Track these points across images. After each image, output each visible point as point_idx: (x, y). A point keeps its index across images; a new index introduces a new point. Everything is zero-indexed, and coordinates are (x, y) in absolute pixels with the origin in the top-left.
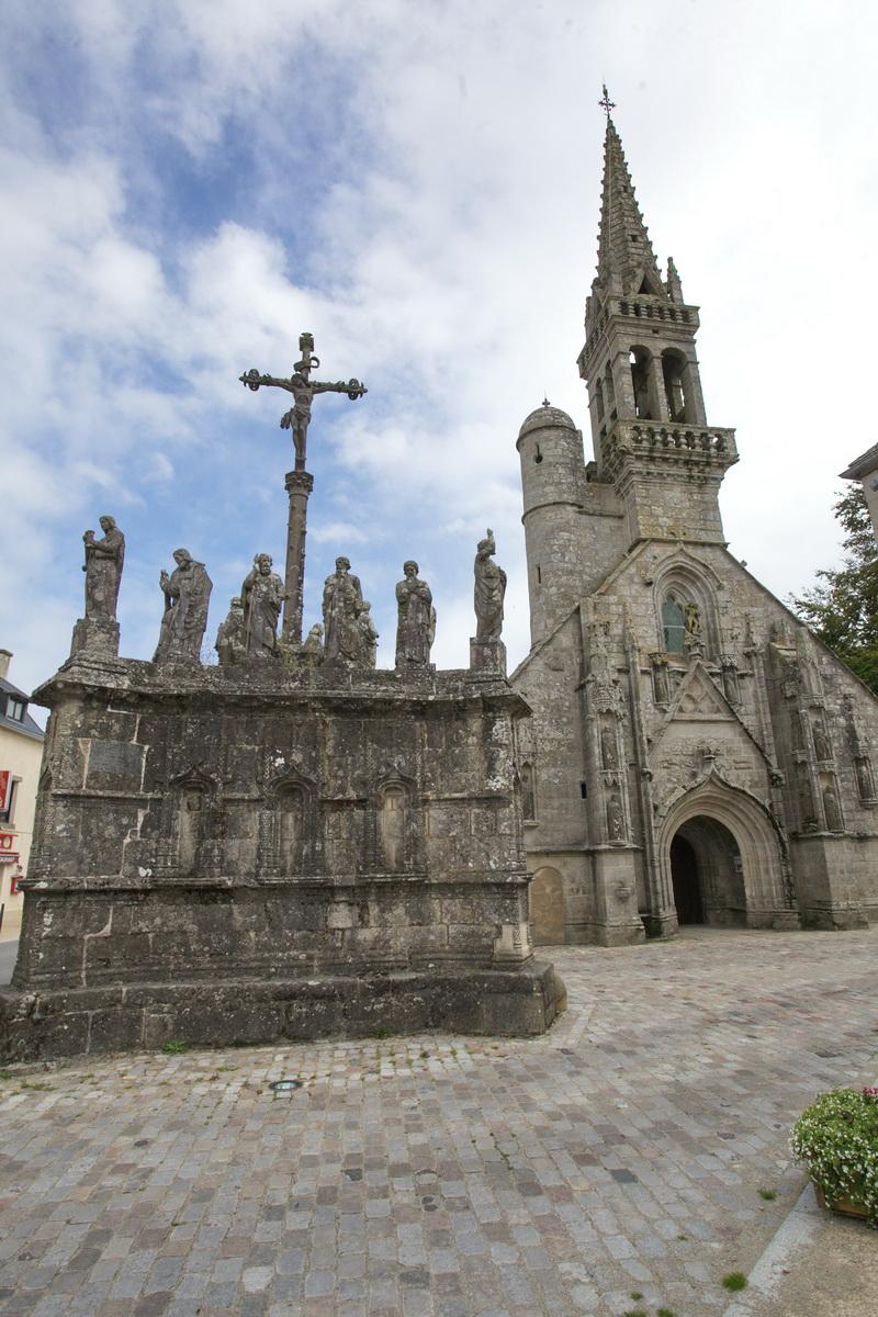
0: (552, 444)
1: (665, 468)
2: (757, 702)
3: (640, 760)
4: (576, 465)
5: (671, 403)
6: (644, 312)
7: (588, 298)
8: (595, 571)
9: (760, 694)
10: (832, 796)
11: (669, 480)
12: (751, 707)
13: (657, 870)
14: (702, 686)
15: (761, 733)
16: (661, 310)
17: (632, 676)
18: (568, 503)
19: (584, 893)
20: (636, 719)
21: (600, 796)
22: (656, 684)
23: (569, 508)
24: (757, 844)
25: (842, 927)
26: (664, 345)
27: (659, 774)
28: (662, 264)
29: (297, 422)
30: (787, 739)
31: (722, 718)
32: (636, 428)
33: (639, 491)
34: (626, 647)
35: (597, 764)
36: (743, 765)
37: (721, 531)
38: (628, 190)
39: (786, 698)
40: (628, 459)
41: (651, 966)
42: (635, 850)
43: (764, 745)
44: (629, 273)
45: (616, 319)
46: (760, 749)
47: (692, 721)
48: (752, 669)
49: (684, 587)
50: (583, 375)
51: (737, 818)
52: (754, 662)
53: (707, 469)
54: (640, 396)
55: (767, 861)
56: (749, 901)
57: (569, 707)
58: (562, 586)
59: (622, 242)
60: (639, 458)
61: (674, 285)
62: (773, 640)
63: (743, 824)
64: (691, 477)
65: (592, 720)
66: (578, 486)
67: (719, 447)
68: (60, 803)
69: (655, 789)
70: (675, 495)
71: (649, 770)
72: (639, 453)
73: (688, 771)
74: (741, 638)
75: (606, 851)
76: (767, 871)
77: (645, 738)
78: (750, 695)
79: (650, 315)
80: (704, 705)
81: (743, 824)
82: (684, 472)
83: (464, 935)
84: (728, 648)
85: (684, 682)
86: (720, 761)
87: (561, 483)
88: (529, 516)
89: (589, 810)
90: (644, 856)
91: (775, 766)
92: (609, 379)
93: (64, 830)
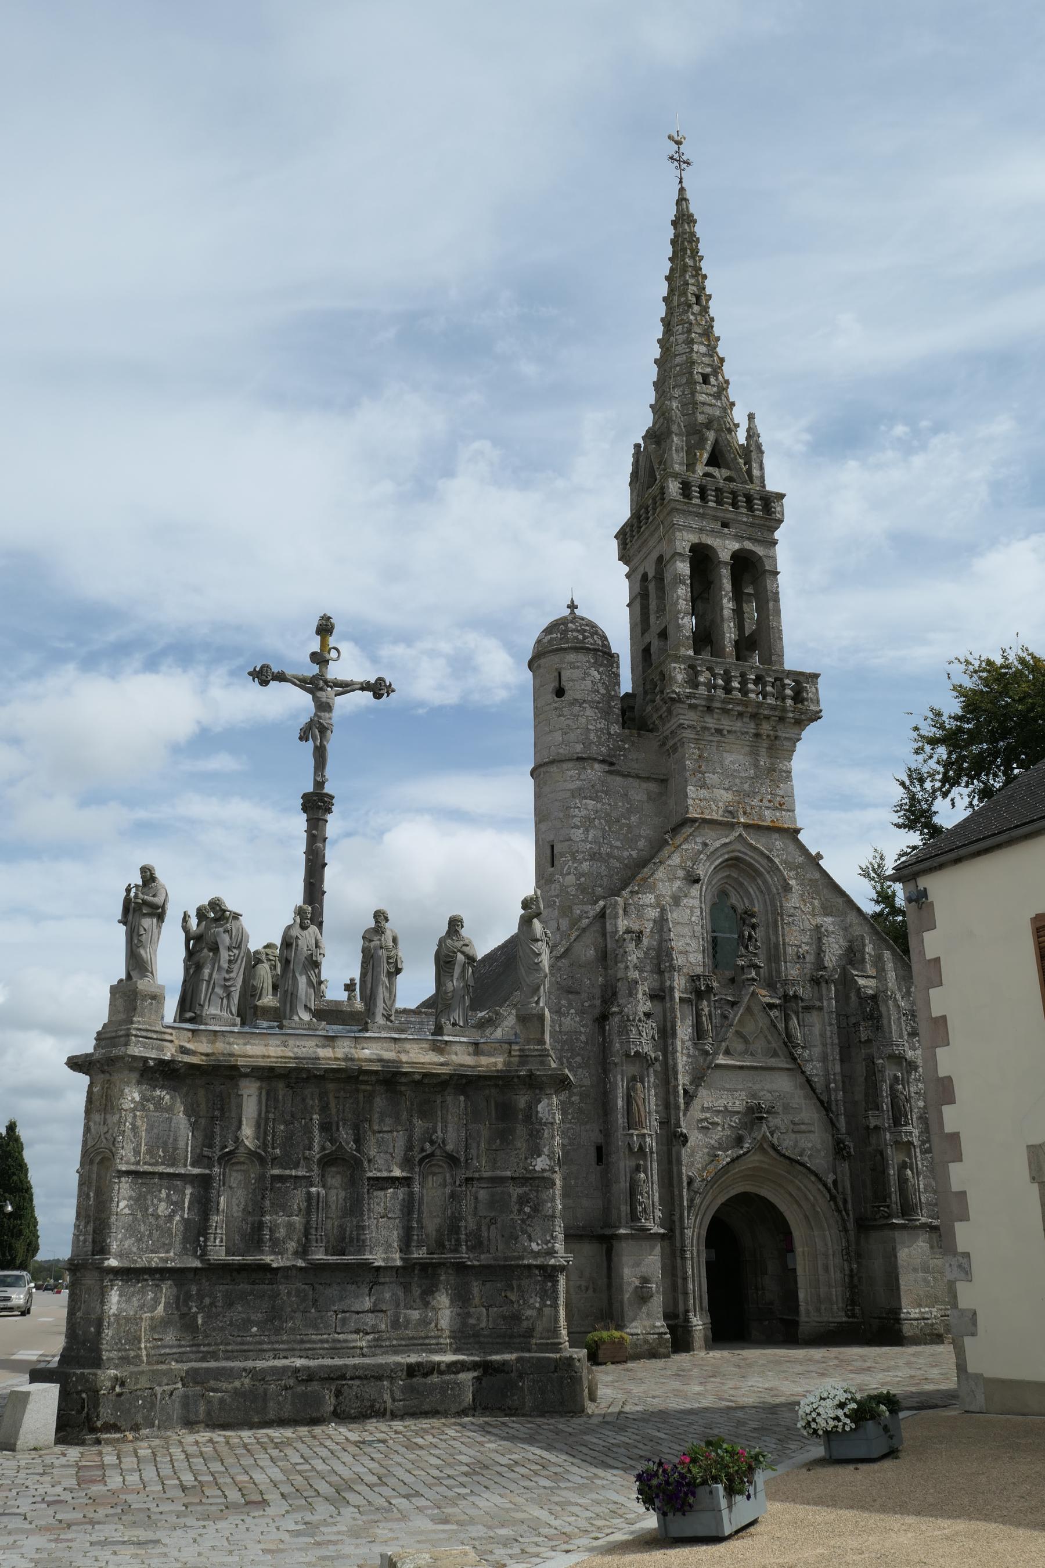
0: (578, 673)
1: (726, 723)
2: (824, 1045)
3: (673, 1117)
4: (608, 703)
5: (739, 613)
6: (711, 496)
7: (637, 446)
8: (626, 854)
9: (828, 1034)
10: (909, 1172)
11: (731, 738)
12: (817, 1051)
13: (689, 1262)
15: (827, 1086)
16: (734, 494)
17: (668, 1005)
18: (595, 759)
19: (594, 1291)
20: (670, 1062)
21: (622, 1165)
22: (698, 1016)
23: (597, 766)
24: (816, 1233)
25: (915, 1341)
26: (736, 546)
27: (695, 1138)
28: (739, 415)
29: (316, 731)
30: (859, 1096)
31: (780, 1065)
33: (691, 751)
34: (661, 960)
35: (620, 1121)
36: (803, 1127)
37: (793, 811)
38: (701, 298)
39: (860, 1041)
40: (678, 708)
41: (679, 1375)
42: (662, 1236)
43: (829, 1102)
44: (695, 433)
45: (673, 505)
46: (825, 1106)
47: (741, 1068)
48: (821, 1000)
49: (741, 884)
50: (624, 558)
51: (791, 1195)
52: (824, 991)
53: (780, 727)
54: (699, 603)
55: (826, 1256)
56: (802, 1308)
57: (586, 1043)
58: (583, 875)
59: (687, 362)
60: (692, 707)
61: (754, 455)
62: (851, 962)
63: (800, 1205)
65: (616, 1064)
66: (609, 734)
67: (798, 696)
68: (123, 1179)
69: (692, 1155)
70: (735, 758)
71: (685, 1131)
72: (693, 701)
74: (810, 958)
75: (626, 1236)
76: (826, 1269)
77: (680, 1087)
78: (815, 1034)
79: (719, 502)
80: (759, 1045)
81: (800, 1205)
82: (751, 728)
83: (504, 1318)
84: (793, 972)
85: (736, 1015)
86: (774, 1121)
87: (590, 726)
88: (543, 769)
89: (606, 1183)
90: (672, 1244)
91: (843, 1130)
92: (660, 578)
93: (127, 1206)
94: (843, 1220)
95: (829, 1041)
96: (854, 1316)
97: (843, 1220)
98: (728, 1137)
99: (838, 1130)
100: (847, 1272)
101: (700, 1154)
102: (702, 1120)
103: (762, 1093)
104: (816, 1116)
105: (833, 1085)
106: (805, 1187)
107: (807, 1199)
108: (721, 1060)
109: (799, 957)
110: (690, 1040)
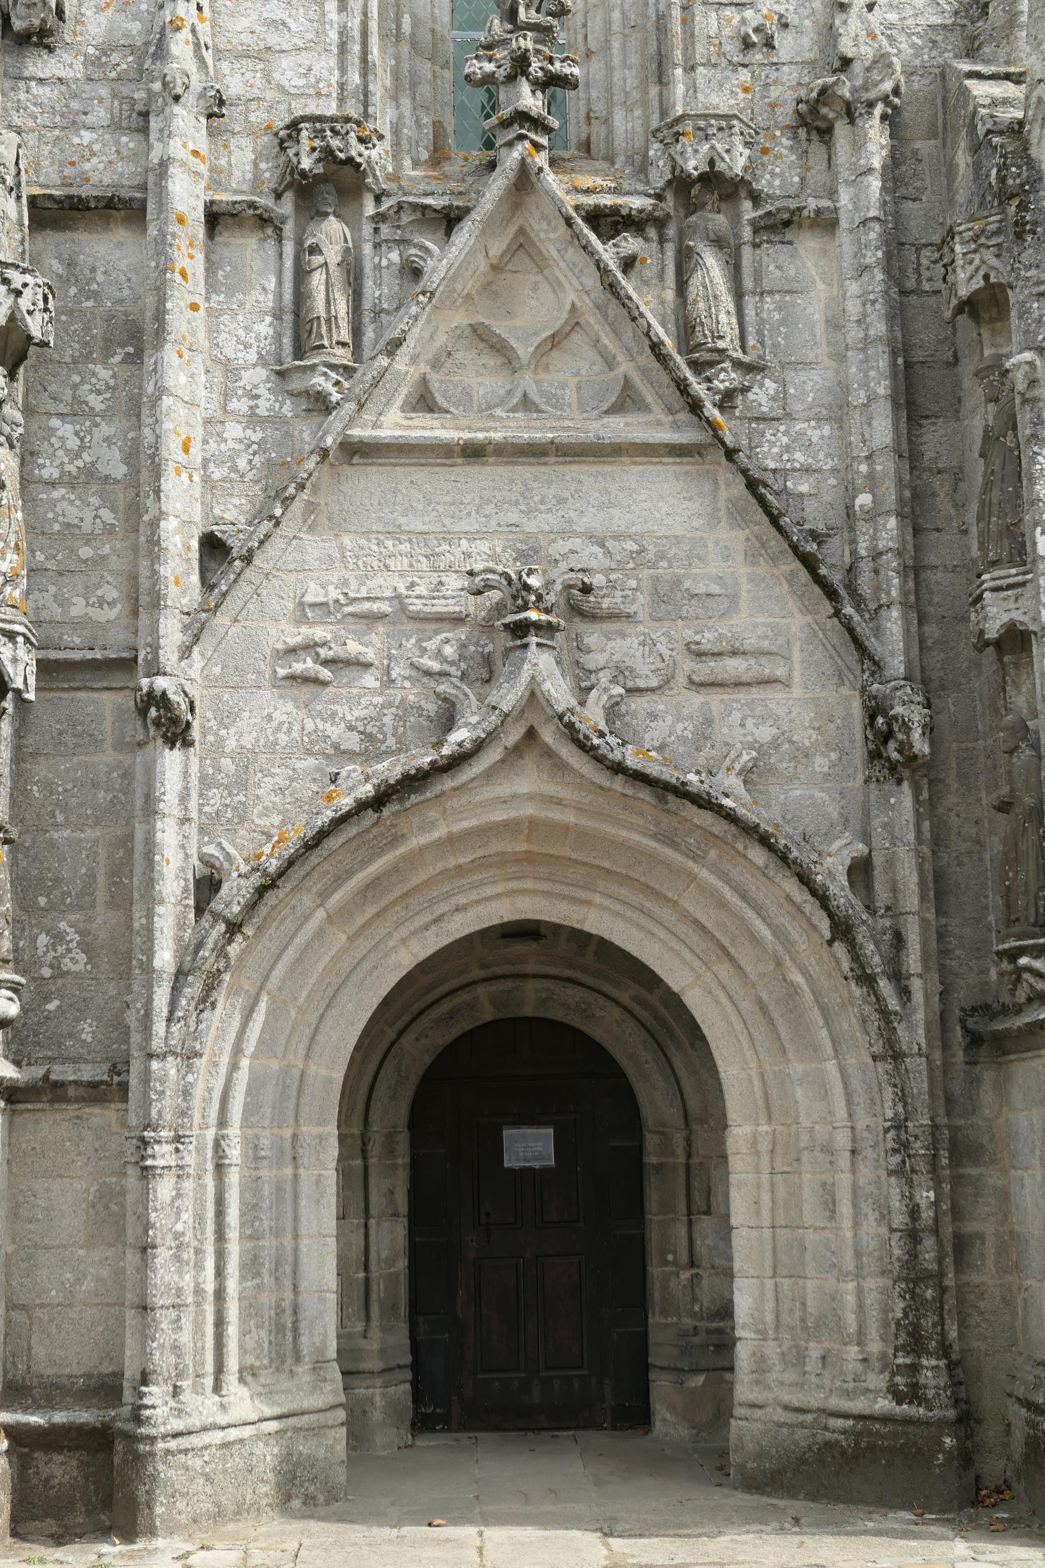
9: (853, 308)
14: (556, 286)
22: (301, 274)
36: (734, 667)
46: (830, 587)
85: (446, 259)
91: (896, 666)
94: (885, 1013)
95: (854, 333)
96: (914, 1394)
97: (885, 1013)
98: (405, 709)
99: (877, 666)
100: (899, 1220)
101: (280, 776)
102: (292, 651)
103: (561, 547)
104: (797, 623)
105: (864, 499)
106: (738, 889)
107: (755, 940)
108: (392, 424)
109: (747, 45)
110: (262, 360)
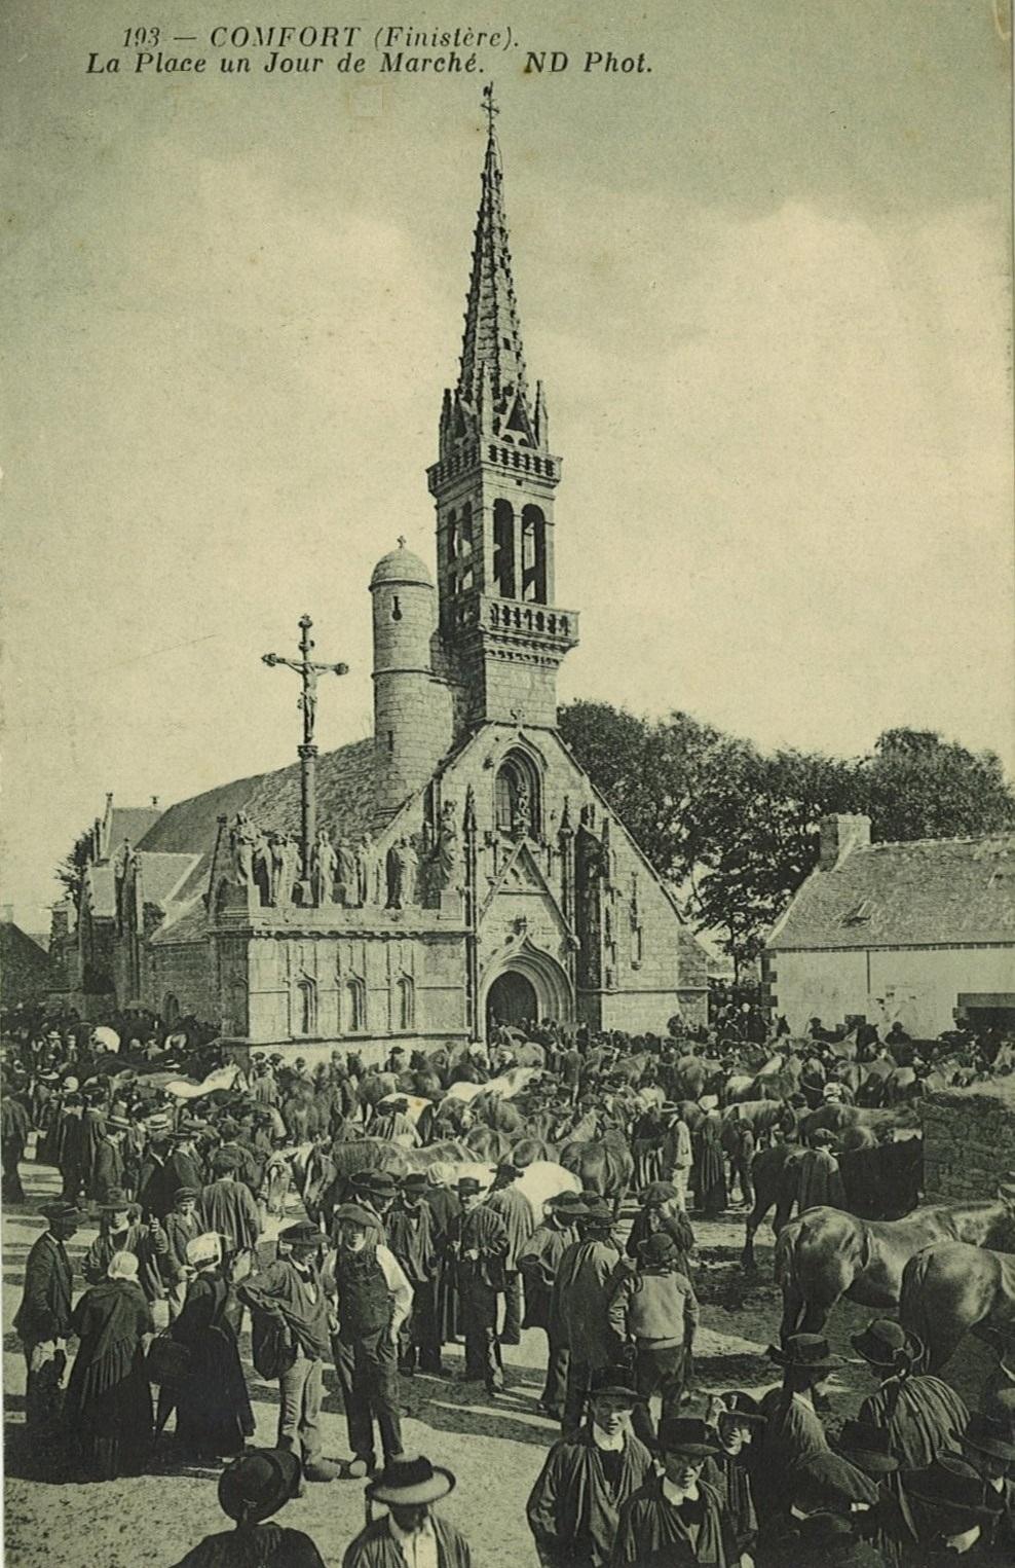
32: (496, 606)
60: (494, 637)
64: (536, 658)
73: (504, 936)
86: (530, 927)
